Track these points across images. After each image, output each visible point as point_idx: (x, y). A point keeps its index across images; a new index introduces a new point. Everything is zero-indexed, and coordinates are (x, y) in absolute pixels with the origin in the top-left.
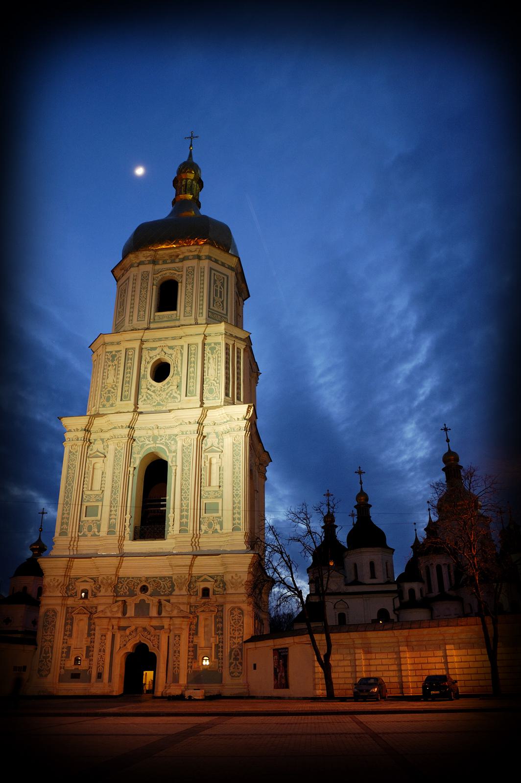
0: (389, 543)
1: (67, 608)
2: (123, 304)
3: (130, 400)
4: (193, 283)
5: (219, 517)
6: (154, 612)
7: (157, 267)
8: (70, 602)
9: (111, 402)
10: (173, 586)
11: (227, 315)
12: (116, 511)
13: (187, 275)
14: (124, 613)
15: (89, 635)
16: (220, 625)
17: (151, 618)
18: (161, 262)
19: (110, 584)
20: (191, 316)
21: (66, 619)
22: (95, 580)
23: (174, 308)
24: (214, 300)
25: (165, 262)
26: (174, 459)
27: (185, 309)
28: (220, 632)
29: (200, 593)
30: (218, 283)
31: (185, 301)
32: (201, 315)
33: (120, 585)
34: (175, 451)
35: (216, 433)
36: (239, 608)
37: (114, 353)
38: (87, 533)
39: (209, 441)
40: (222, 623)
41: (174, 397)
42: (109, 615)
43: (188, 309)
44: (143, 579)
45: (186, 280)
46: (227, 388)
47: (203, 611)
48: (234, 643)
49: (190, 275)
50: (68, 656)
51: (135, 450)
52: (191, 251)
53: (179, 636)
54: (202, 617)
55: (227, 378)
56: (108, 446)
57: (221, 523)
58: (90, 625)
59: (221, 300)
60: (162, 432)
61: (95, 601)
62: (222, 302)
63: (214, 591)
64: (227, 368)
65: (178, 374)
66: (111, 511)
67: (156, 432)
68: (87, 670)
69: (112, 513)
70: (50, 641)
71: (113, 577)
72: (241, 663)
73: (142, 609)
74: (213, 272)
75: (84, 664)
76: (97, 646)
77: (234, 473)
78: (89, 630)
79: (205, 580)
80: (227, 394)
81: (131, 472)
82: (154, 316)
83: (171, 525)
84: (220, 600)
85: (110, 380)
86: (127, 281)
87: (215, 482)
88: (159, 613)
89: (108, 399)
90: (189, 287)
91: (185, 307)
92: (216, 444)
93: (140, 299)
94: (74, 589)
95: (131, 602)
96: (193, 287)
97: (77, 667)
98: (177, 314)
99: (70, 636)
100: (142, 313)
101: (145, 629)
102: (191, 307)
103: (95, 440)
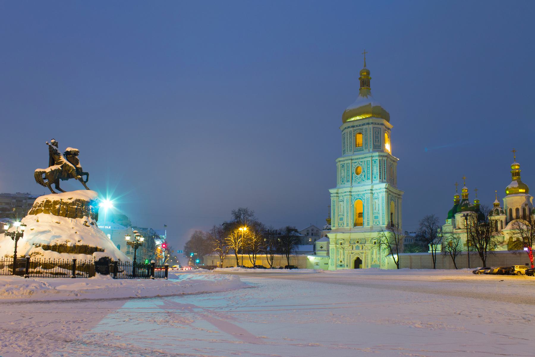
6: (361, 248)
7: (354, 128)
25: (357, 126)
30: (377, 133)
39: (376, 195)
46: (380, 176)
51: (353, 199)
55: (380, 172)
60: (360, 193)
64: (380, 169)
67: (358, 193)
75: (342, 263)
80: (380, 178)
85: (343, 175)
87: (377, 209)
95: (354, 246)
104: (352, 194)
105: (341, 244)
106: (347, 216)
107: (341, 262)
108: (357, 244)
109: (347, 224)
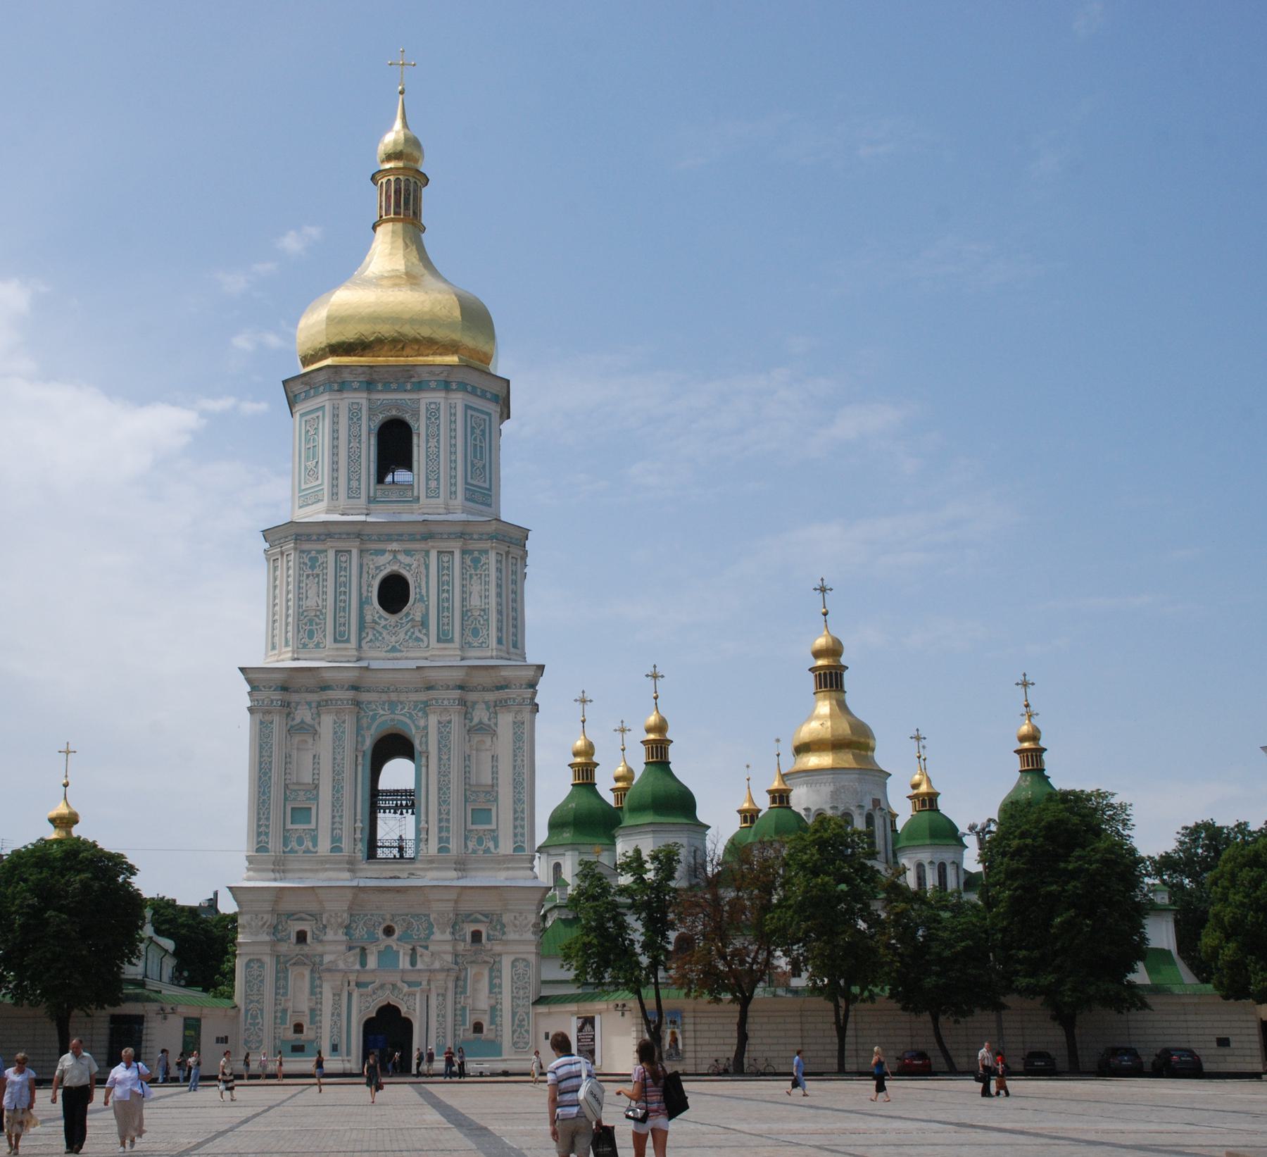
0: (702, 815)
1: (278, 956)
3: (348, 641)
5: (493, 831)
6: (404, 963)
8: (283, 948)
9: (315, 639)
10: (431, 926)
11: (490, 490)
12: (341, 817)
14: (363, 963)
15: (312, 993)
16: (497, 981)
17: (403, 971)
18: (380, 387)
19: (340, 925)
21: (277, 972)
22: (315, 917)
24: (473, 465)
25: (387, 388)
28: (497, 990)
29: (469, 938)
30: (478, 431)
33: (354, 925)
34: (426, 727)
35: (486, 703)
36: (524, 960)
37: (313, 554)
38: (297, 848)
40: (500, 977)
41: (418, 639)
42: (341, 965)
43: (433, 484)
44: (388, 916)
47: (472, 962)
48: (518, 1006)
50: (284, 1021)
51: (364, 722)
52: (431, 373)
53: (444, 995)
54: (471, 971)
56: (319, 715)
57: (496, 840)
58: (312, 980)
59: (480, 464)
60: (403, 697)
61: (320, 949)
62: (484, 466)
63: (488, 935)
65: (421, 600)
66: (333, 817)
67: (394, 696)
68: (313, 1041)
69: (337, 819)
70: (258, 1001)
71: (345, 915)
72: (527, 1031)
73: (388, 956)
74: (469, 412)
76: (327, 1008)
77: (514, 767)
78: (313, 987)
79: (477, 921)
81: (360, 759)
82: (375, 491)
84: (498, 948)
86: (320, 413)
88: (413, 963)
89: (311, 635)
90: (433, 443)
91: (428, 479)
92: (486, 720)
96: (438, 441)
97: (298, 1036)
99: (285, 994)
100: (354, 484)
101: (394, 986)
102: (438, 479)
103: (298, 703)
104: (364, 697)
105: (301, 937)
106: (336, 803)
107: (298, 1028)
108: (386, 942)
109: (336, 839)
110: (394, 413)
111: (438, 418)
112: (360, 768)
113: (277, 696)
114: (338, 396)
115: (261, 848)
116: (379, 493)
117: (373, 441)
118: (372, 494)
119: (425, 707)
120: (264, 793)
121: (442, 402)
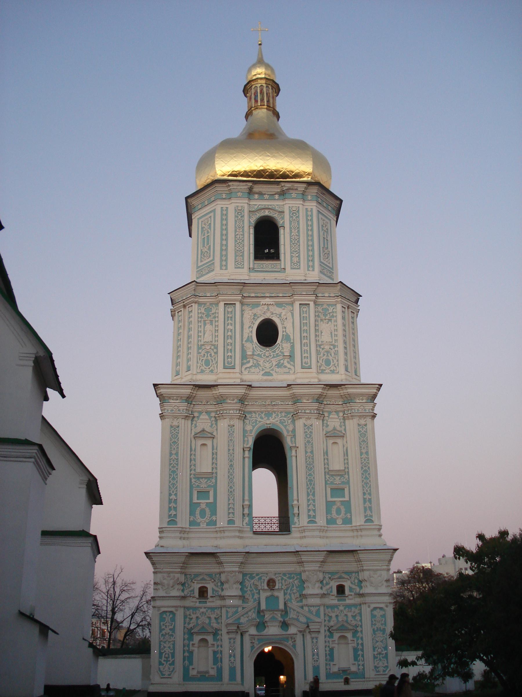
2: (208, 243)
4: (298, 228)
7: (252, 203)
13: (290, 217)
20: (299, 268)
23: (275, 256)
26: (293, 439)
27: (291, 260)
31: (291, 250)
32: (311, 269)
43: (295, 260)
45: (290, 224)
49: (294, 218)
53: (317, 638)
81: (247, 453)
82: (254, 265)
83: (296, 515)
91: (292, 257)
93: (236, 241)
94: (191, 587)
96: (298, 231)
98: (280, 264)
102: (299, 257)
110: (267, 213)
111: (298, 217)
112: (247, 460)
113: (183, 406)
114: (227, 202)
115: (172, 521)
116: (255, 266)
117: (252, 231)
118: (251, 266)
119: (295, 416)
120: (174, 479)
121: (301, 206)
